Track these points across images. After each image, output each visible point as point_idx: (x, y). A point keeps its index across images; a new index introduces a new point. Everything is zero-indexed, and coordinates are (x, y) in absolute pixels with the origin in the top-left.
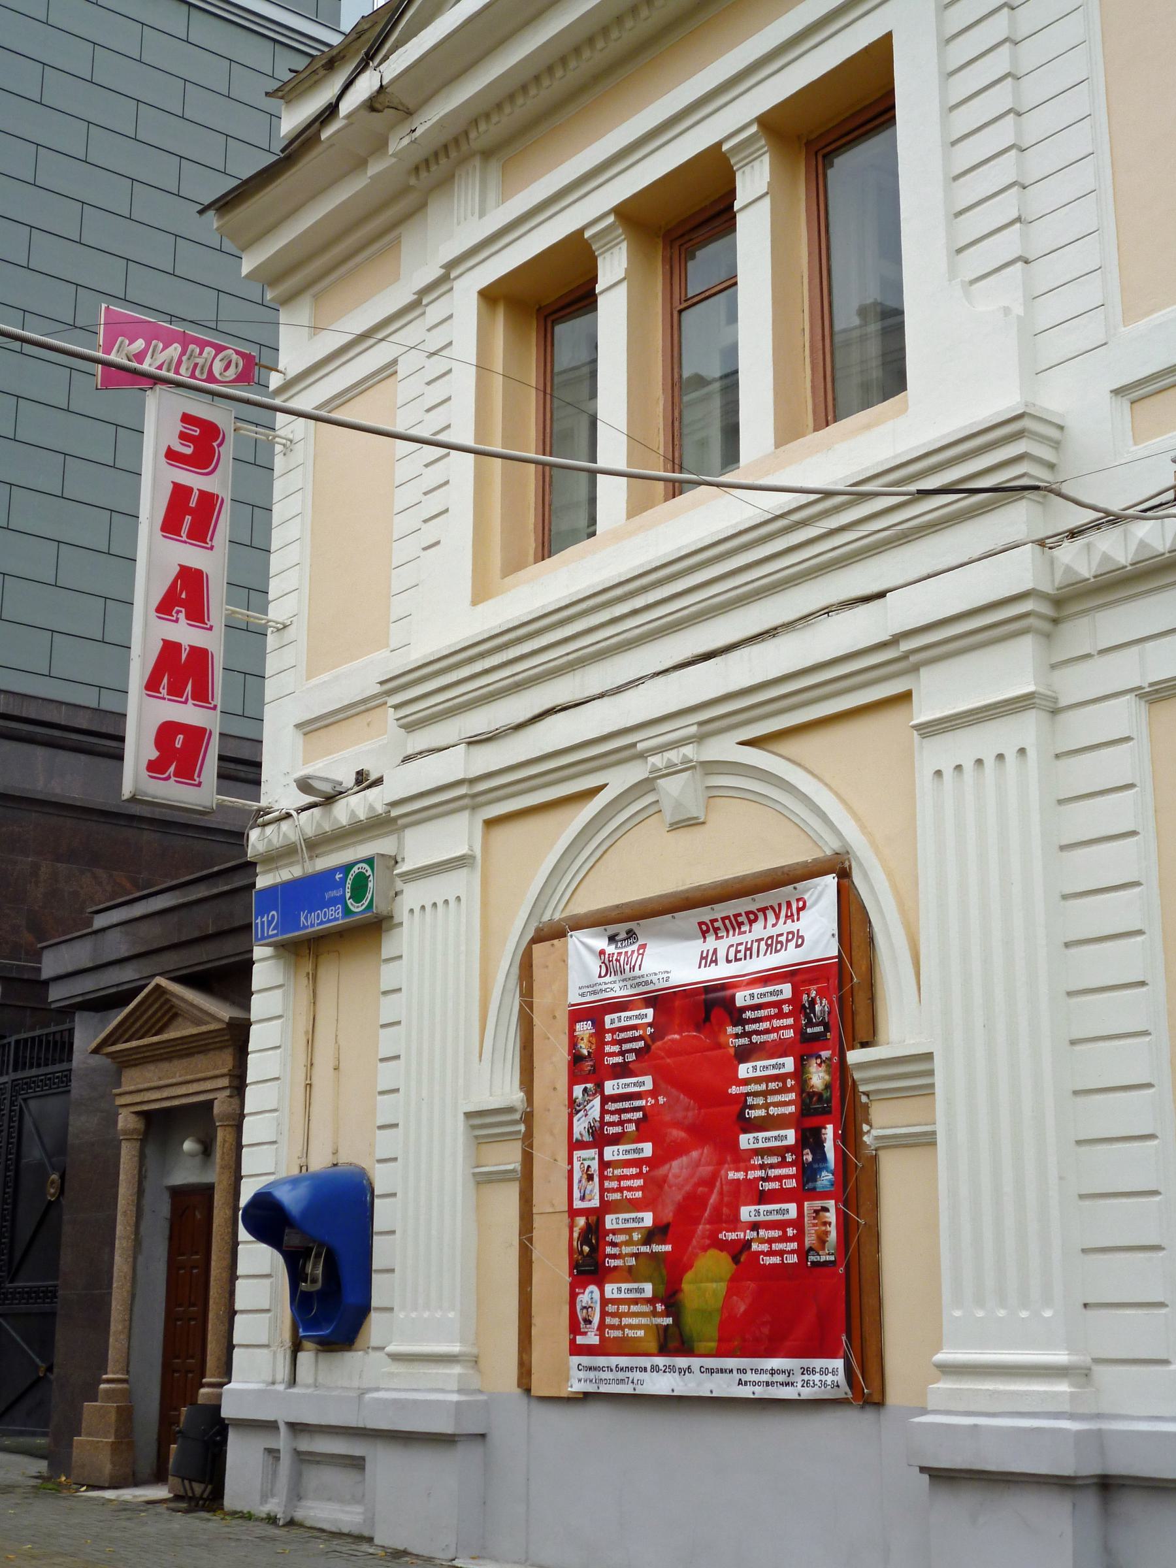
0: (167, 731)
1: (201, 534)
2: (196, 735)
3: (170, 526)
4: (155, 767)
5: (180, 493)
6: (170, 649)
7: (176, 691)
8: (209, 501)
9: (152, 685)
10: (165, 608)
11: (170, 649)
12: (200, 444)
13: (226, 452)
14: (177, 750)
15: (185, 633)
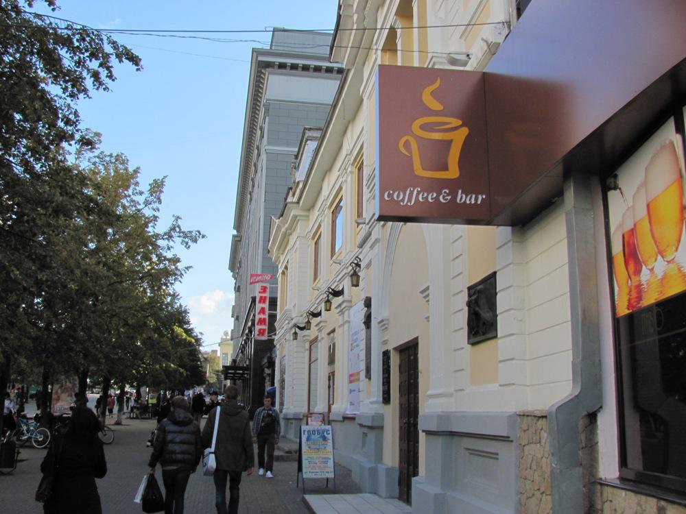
0: (260, 330)
1: (264, 302)
2: (264, 330)
3: (260, 302)
4: (258, 335)
5: (261, 297)
6: (260, 319)
7: (261, 324)
8: (265, 298)
9: (258, 324)
10: (259, 313)
11: (260, 319)
12: (264, 289)
13: (268, 290)
14: (261, 332)
15: (262, 316)
